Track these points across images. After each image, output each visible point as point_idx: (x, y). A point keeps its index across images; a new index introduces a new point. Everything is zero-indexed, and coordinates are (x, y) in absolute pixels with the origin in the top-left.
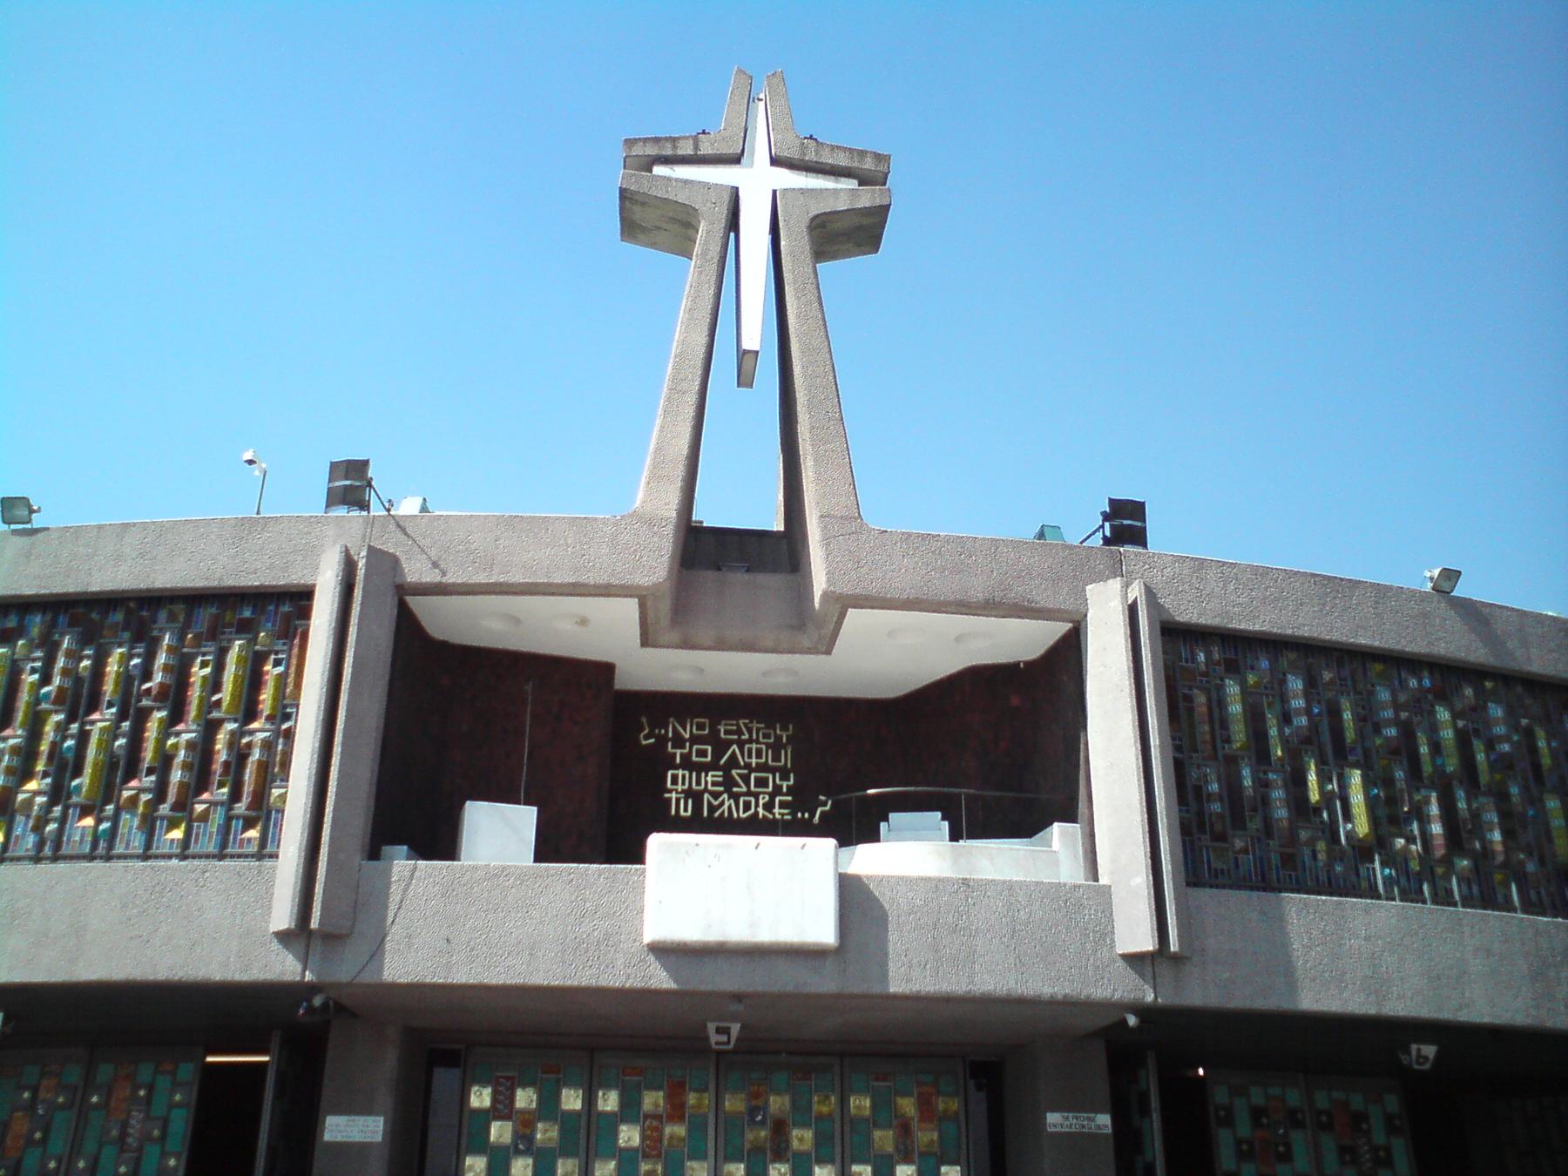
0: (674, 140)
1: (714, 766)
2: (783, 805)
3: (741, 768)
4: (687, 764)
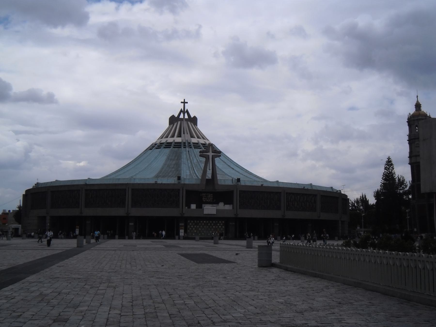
1: (206, 197)
4: (204, 197)
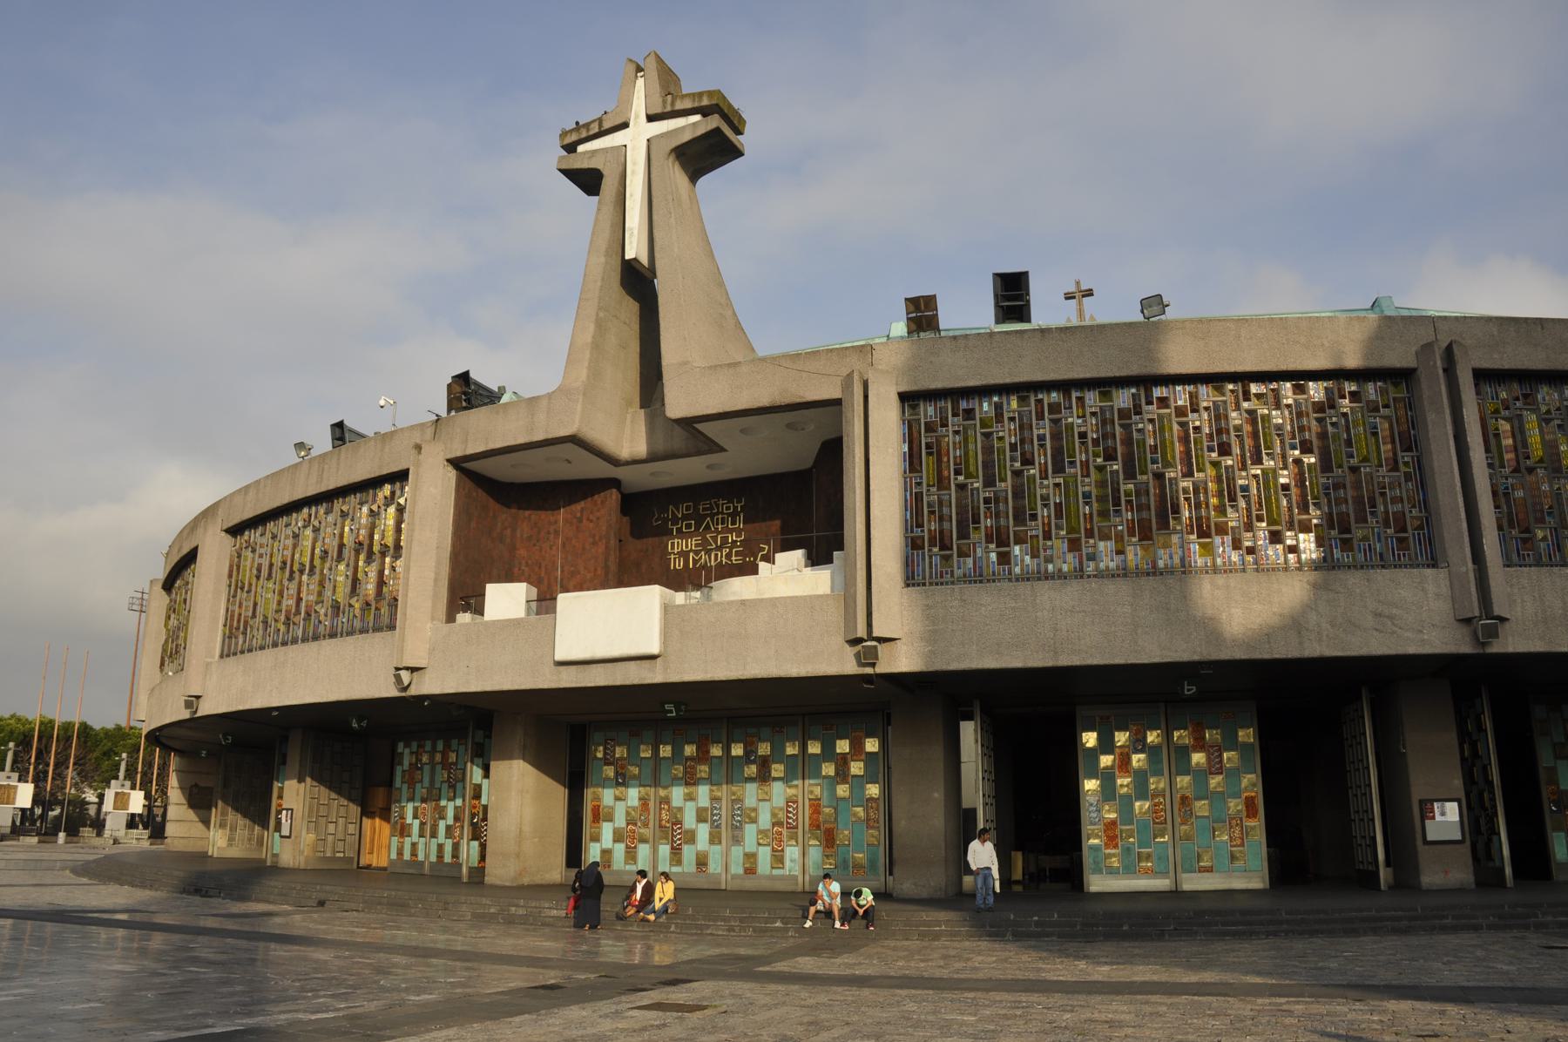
0: (587, 126)
2: (737, 554)
3: (712, 532)
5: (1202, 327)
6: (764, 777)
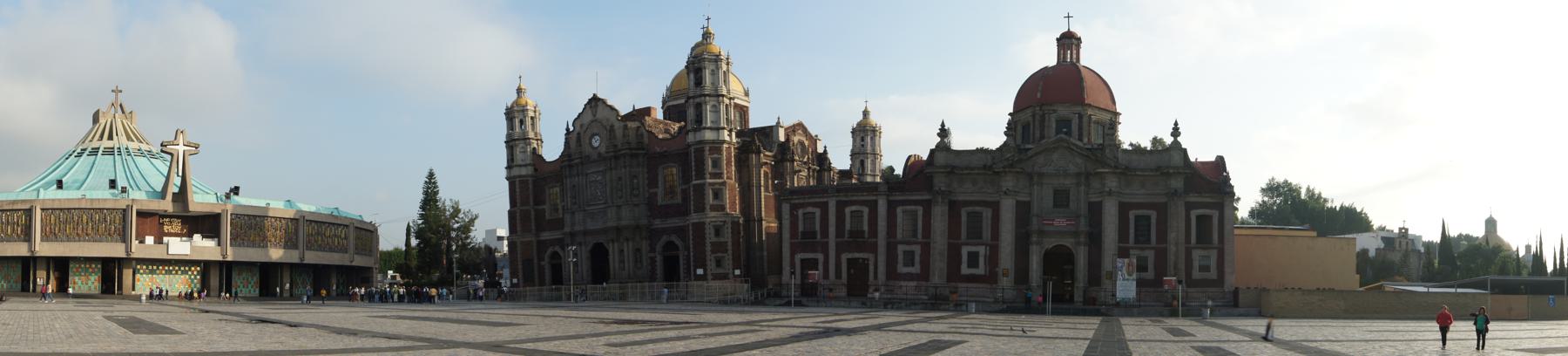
5: (274, 209)
6: (177, 273)
